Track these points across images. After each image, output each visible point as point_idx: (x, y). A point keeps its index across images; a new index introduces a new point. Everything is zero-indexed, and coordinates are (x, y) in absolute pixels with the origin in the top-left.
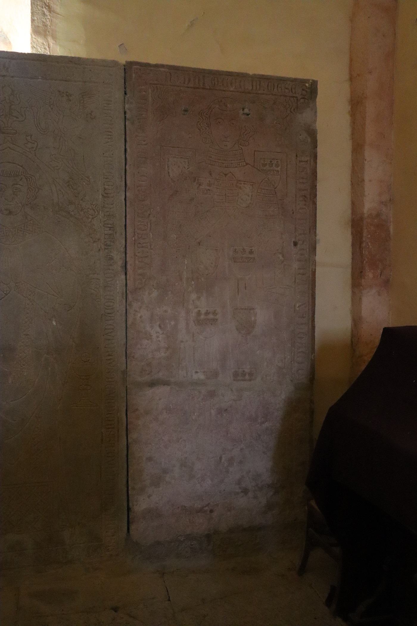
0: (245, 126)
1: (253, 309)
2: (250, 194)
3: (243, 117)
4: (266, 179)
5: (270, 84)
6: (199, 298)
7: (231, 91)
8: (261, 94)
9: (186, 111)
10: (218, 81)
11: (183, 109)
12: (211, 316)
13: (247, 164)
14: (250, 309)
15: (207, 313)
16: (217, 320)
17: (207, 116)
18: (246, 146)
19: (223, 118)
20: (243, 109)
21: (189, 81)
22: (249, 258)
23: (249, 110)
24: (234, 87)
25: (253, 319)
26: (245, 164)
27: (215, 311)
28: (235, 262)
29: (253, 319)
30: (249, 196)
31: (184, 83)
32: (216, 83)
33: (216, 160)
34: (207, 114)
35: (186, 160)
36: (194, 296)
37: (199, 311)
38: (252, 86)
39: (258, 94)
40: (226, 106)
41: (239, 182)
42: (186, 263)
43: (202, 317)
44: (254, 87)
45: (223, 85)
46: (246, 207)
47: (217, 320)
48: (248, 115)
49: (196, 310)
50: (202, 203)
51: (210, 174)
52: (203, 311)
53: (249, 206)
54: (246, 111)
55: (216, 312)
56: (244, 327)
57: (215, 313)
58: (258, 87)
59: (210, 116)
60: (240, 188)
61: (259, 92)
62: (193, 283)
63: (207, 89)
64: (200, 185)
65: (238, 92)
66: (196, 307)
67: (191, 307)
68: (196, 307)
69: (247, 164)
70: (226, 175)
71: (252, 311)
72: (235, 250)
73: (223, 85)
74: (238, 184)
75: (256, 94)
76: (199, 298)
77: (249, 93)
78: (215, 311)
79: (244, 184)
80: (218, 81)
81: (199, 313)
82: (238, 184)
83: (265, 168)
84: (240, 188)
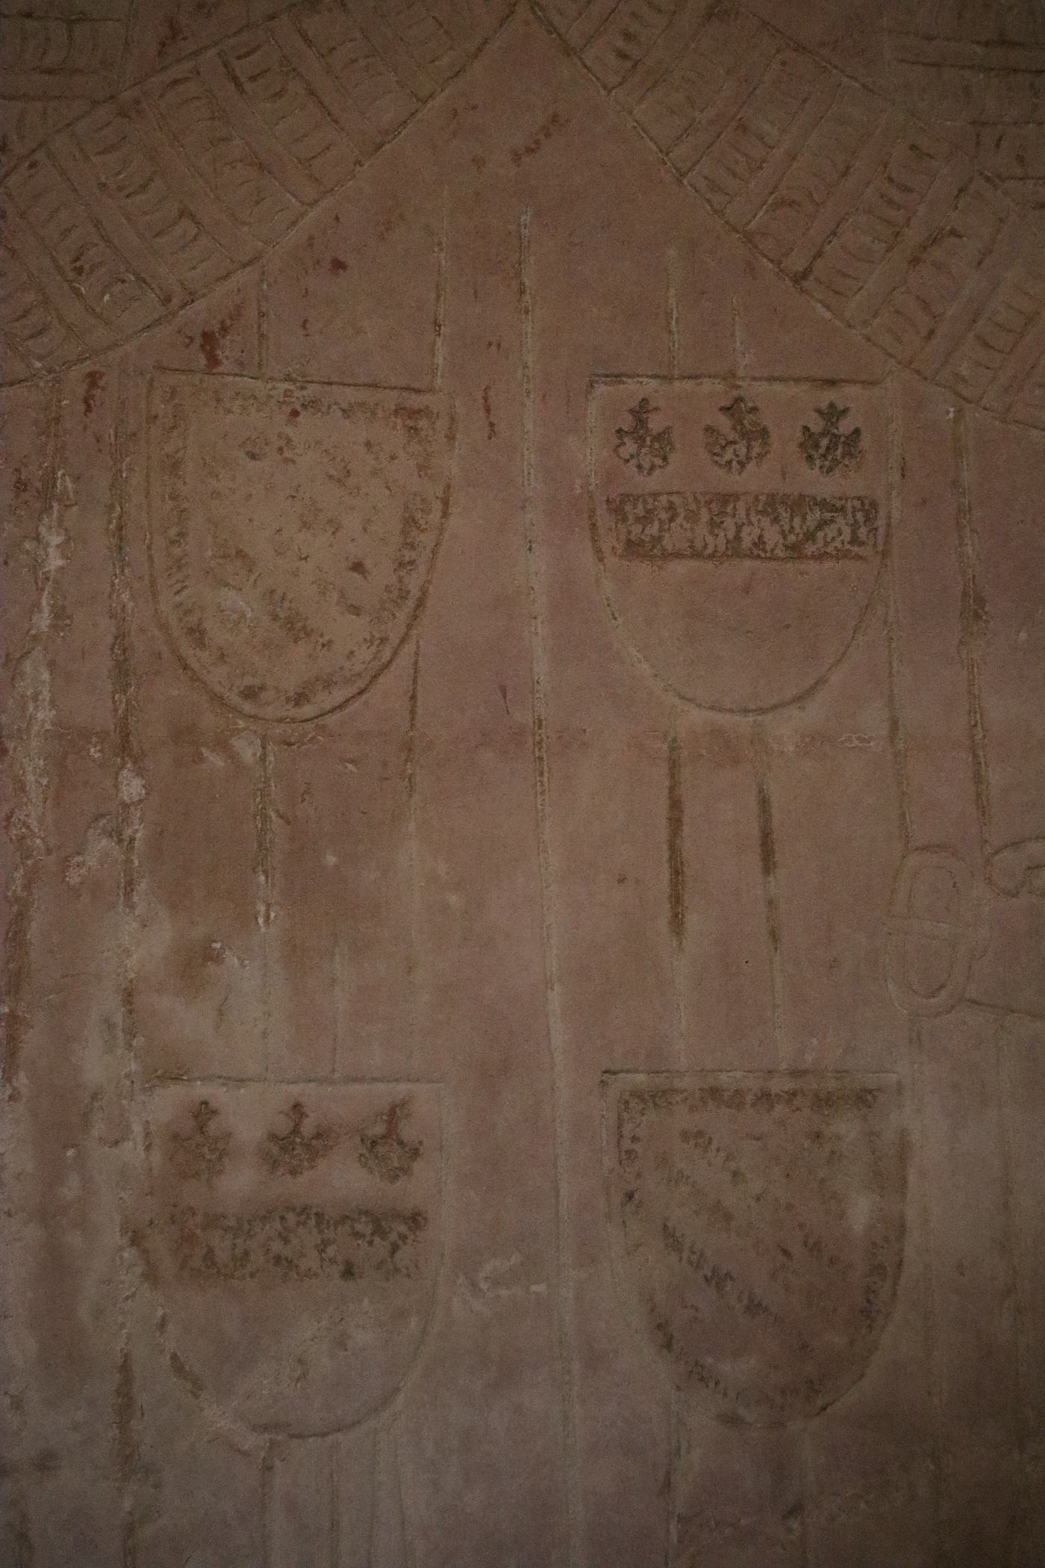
1: (864, 1098)
6: (194, 965)
12: (344, 1178)
14: (824, 1102)
15: (295, 1142)
16: (416, 1220)
22: (799, 504)
25: (861, 1211)
27: (394, 1114)
28: (634, 549)
29: (861, 1211)
36: (139, 940)
37: (204, 1112)
42: (55, 562)
43: (240, 1182)
47: (416, 1220)
49: (165, 1105)
52: (248, 1116)
55: (408, 1131)
56: (754, 1307)
57: (388, 1140)
62: (132, 787)
66: (168, 1070)
67: (97, 1064)
68: (168, 1070)
71: (846, 1127)
72: (641, 411)
76: (194, 965)
78: (394, 1114)
81: (198, 1140)
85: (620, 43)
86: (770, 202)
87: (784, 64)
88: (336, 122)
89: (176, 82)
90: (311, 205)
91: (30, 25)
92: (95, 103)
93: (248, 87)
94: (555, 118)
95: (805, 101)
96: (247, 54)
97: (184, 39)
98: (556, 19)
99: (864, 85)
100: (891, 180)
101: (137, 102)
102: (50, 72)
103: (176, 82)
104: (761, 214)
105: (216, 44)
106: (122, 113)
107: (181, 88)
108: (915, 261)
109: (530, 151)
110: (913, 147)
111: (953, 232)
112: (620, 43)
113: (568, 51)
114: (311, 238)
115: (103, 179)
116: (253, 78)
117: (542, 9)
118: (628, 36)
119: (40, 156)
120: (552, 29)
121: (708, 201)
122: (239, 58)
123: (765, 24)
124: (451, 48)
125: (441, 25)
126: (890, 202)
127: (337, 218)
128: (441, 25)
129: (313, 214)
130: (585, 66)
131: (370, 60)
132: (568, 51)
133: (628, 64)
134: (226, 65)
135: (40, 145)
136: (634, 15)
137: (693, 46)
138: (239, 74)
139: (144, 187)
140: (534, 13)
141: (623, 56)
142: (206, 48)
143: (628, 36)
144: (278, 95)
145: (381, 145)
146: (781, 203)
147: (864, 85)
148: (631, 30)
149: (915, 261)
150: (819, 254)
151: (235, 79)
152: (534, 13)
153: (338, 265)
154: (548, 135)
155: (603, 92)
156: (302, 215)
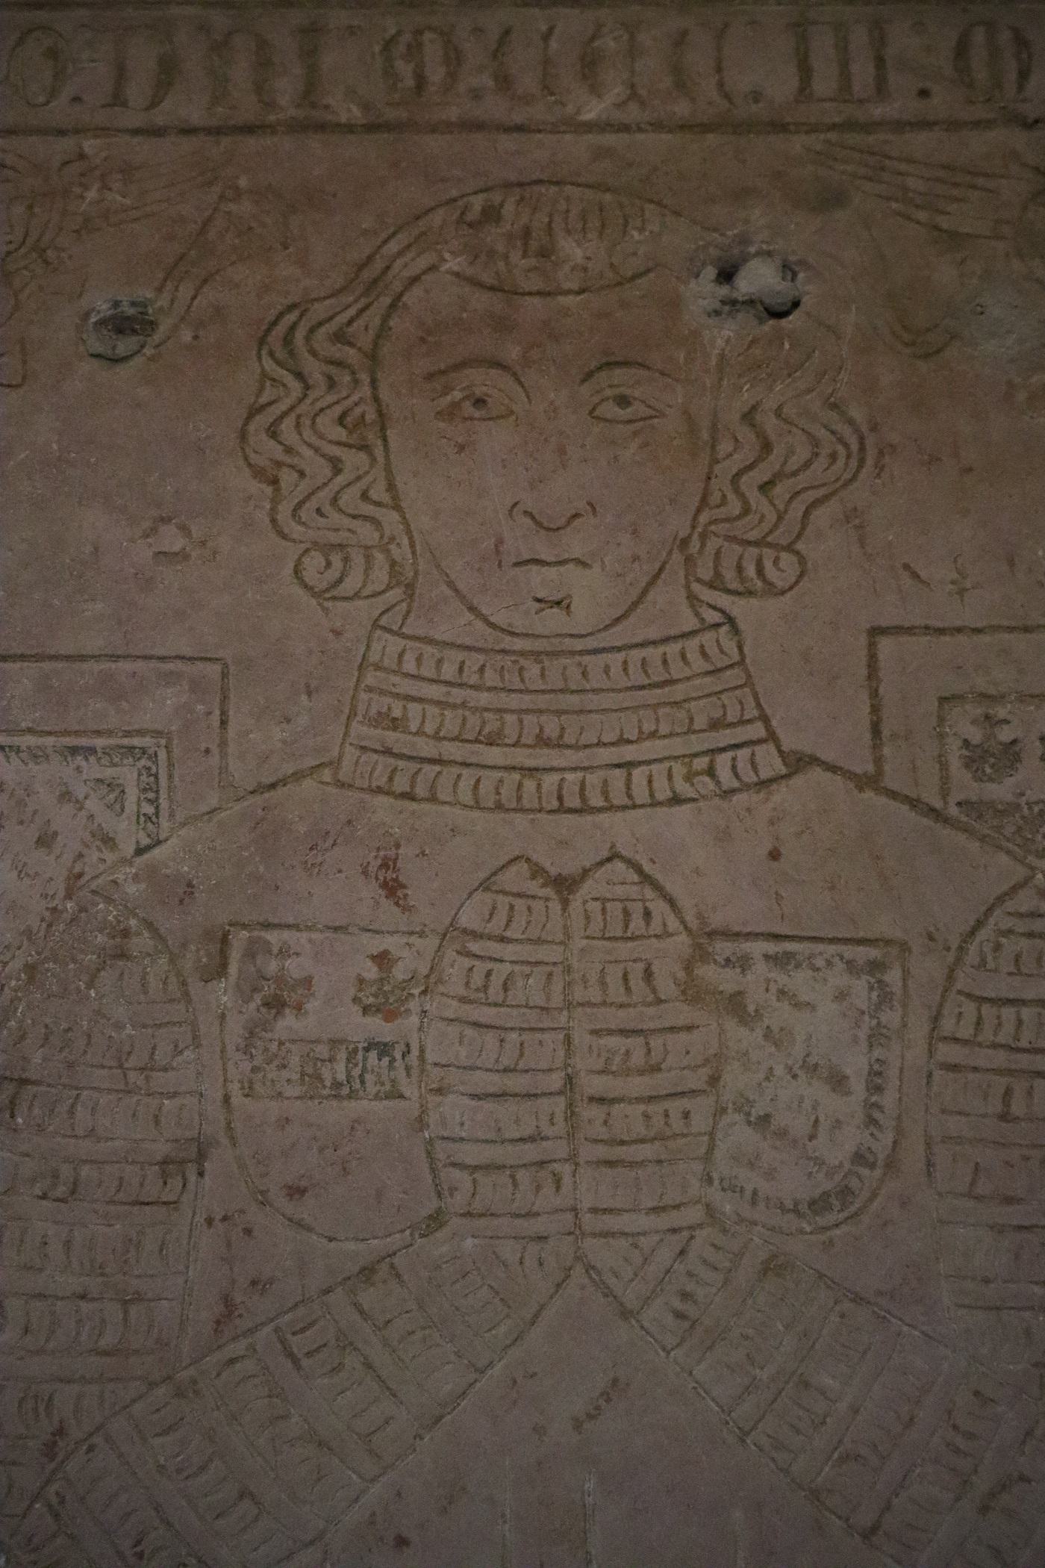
0: (748, 417)
2: (855, 1064)
3: (723, 335)
4: (1025, 901)
5: (979, 36)
7: (589, 127)
8: (900, 126)
9: (121, 325)
10: (454, 58)
11: (104, 308)
13: (798, 763)
17: (351, 354)
18: (772, 590)
19: (513, 353)
20: (726, 275)
21: (168, 72)
23: (788, 270)
24: (616, 92)
26: (770, 762)
30: (838, 1082)
31: (118, 100)
32: (436, 74)
33: (452, 750)
34: (339, 337)
35: (128, 775)
38: (805, 72)
39: (869, 127)
40: (544, 253)
41: (723, 948)
44: (824, 83)
45: (504, 82)
46: (819, 1204)
48: (780, 315)
50: (296, 1192)
51: (393, 889)
53: (845, 1193)
54: (759, 278)
58: (863, 72)
59: (373, 357)
60: (735, 1005)
61: (878, 111)
63: (349, 128)
64: (276, 1005)
65: (658, 126)
69: (798, 763)
70: (565, 885)
73: (504, 82)
74: (707, 972)
75: (850, 125)
77: (779, 127)
79: (779, 961)
80: (454, 58)
82: (707, 972)
83: (1000, 791)
84: (735, 1005)
85: (677, 1304)
86: (836, 1455)
87: (842, 1316)
88: (394, 1396)
89: (232, 1361)
90: (372, 1480)
91: (85, 1306)
92: (153, 1385)
93: (305, 1362)
94: (615, 1381)
95: (865, 1353)
96: (303, 1330)
97: (240, 1316)
98: (612, 1281)
99: (923, 1332)
100: (955, 1427)
101: (195, 1382)
102: (106, 1353)
103: (232, 1361)
104: (827, 1469)
105: (272, 1320)
106: (179, 1394)
107: (238, 1366)
108: (984, 1509)
109: (590, 1417)
110: (977, 1393)
111: (1023, 1478)
112: (677, 1304)
113: (626, 1314)
114: (373, 1514)
115: (162, 1462)
116: (309, 1354)
117: (599, 1273)
118: (685, 1296)
119: (97, 1440)
120: (609, 1293)
121: (773, 1459)
122: (294, 1334)
123: (821, 1276)
124: (508, 1316)
125: (497, 1293)
126: (957, 1451)
127: (399, 1494)
128: (497, 1293)
129: (376, 1489)
130: (642, 1327)
131: (427, 1332)
132: (626, 1314)
133: (686, 1324)
134: (283, 1342)
135: (98, 1429)
136: (690, 1274)
137: (750, 1302)
138: (295, 1350)
139: (203, 1468)
140: (590, 1277)
141: (680, 1315)
142: (263, 1324)
143: (685, 1296)
144: (336, 1370)
145: (442, 1417)
146: (844, 1459)
147: (923, 1332)
148: (688, 1289)
149: (984, 1509)
150: (888, 1507)
151: (291, 1355)
152: (590, 1277)
153: (402, 1542)
154: (608, 1400)
155: (662, 1353)
156: (364, 1491)
